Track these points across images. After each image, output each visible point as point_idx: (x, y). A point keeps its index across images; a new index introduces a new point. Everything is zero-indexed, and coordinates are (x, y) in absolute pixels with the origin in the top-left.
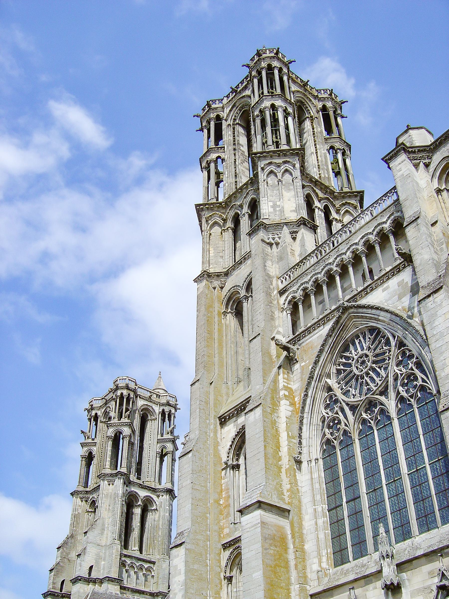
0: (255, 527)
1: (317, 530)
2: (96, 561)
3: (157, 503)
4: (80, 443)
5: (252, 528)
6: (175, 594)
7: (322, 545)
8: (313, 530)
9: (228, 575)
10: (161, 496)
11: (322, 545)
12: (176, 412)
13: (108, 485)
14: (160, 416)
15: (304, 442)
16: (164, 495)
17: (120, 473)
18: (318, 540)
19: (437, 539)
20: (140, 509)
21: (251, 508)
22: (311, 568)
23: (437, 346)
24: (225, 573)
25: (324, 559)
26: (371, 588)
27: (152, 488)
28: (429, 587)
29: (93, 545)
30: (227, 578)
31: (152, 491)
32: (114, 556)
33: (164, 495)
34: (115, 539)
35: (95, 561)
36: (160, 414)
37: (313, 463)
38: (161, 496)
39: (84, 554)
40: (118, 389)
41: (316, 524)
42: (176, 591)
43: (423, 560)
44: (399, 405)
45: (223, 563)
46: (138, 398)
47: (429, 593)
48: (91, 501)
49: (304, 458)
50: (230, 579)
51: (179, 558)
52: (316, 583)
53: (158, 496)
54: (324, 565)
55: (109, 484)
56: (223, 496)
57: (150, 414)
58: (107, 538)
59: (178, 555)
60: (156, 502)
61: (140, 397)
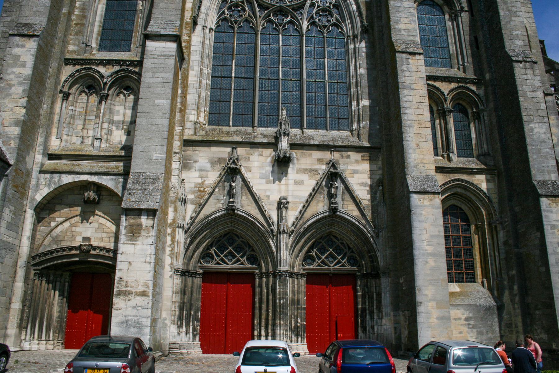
0: (167, 57)
1: (200, 87)
5: (162, 57)
6: (10, 86)
7: (202, 102)
8: (196, 85)
9: (66, 90)
11: (202, 102)
15: (203, 9)
18: (199, 97)
19: (320, 138)
21: (162, 38)
22: (189, 118)
23: (396, 5)
24: (63, 87)
25: (202, 115)
26: (256, 154)
28: (316, 170)
30: (64, 93)
37: (207, 31)
41: (201, 82)
42: (12, 83)
43: (316, 148)
44: (310, 27)
45: (63, 78)
47: (315, 174)
49: (200, 21)
50: (66, 96)
51: (24, 49)
52: (191, 132)
54: (201, 119)
56: (76, 13)
59: (23, 46)
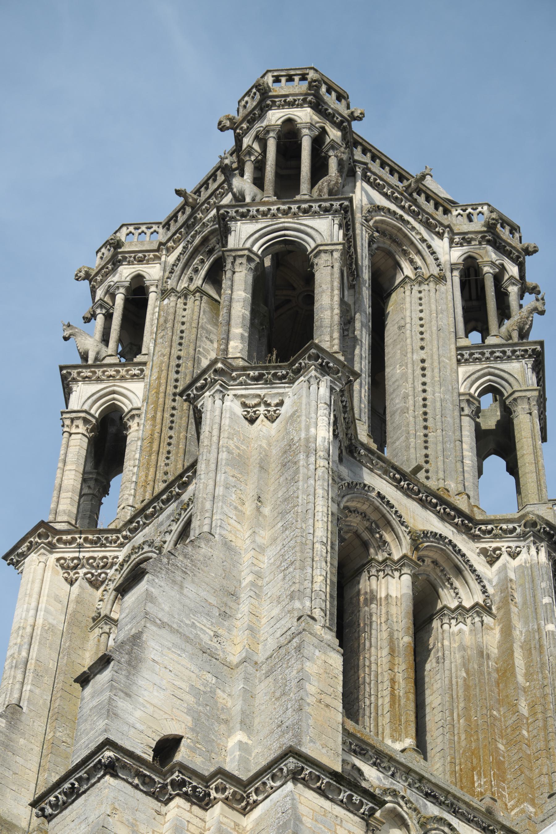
2: (197, 720)
4: (62, 368)
10: (505, 557)
16: (524, 550)
17: (317, 357)
20: (407, 579)
27: (460, 513)
29: (176, 639)
32: (311, 688)
33: (524, 550)
34: (313, 619)
36: (456, 273)
38: (505, 557)
39: (129, 663)
40: (269, 108)
55: (252, 421)
58: (252, 630)
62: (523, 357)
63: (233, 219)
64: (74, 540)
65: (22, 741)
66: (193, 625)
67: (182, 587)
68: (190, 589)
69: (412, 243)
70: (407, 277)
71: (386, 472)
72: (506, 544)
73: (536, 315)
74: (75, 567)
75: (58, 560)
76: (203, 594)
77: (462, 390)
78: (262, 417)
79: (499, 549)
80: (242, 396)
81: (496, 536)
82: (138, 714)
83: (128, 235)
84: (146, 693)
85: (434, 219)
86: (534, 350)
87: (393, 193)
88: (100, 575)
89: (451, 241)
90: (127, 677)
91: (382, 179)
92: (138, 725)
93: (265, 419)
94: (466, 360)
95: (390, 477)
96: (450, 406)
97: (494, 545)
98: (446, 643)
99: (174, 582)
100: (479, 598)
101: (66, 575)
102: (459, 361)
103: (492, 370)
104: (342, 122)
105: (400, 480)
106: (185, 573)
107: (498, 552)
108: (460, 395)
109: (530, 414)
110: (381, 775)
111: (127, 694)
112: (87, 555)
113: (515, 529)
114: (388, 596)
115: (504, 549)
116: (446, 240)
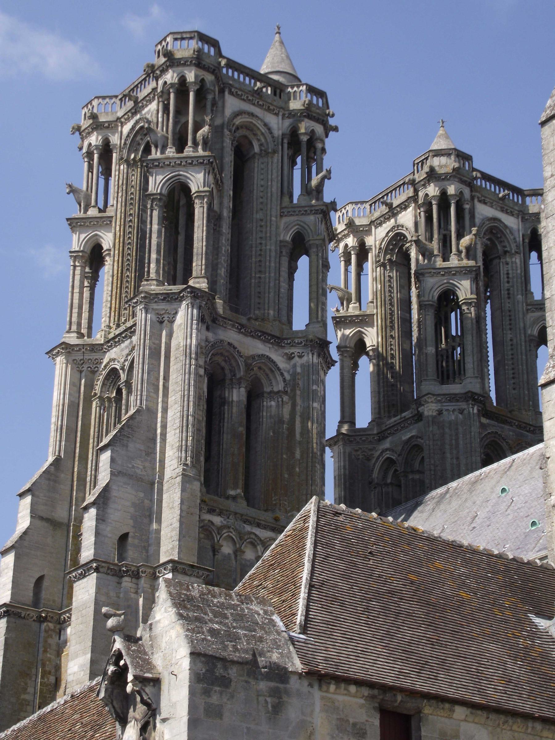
3: (288, 377)
12: (327, 136)
13: (158, 324)
14: (286, 146)
20: (243, 390)
27: (273, 336)
31: (272, 343)
35: (131, 522)
46: (226, 93)
48: (107, 370)
53: (290, 357)
57: (259, 140)
60: (286, 374)
61: (231, 93)
62: (317, 214)
63: (151, 168)
64: (80, 350)
65: (62, 475)
66: (133, 467)
67: (127, 447)
68: (131, 445)
69: (259, 129)
70: (255, 153)
71: (233, 326)
72: (298, 351)
73: (326, 180)
74: (82, 364)
75: (74, 360)
76: (138, 446)
77: (282, 238)
78: (166, 321)
79: (293, 353)
80: (156, 309)
81: (292, 346)
82: (109, 529)
83: (99, 104)
84: (112, 516)
85: (272, 105)
86: (322, 210)
87: (247, 97)
88: (95, 368)
89: (284, 115)
90: (103, 511)
91: (241, 90)
92: (109, 535)
93: (168, 323)
94: (286, 216)
95: (236, 328)
96: (273, 254)
97: (292, 351)
98: (265, 414)
99: (123, 445)
100: (281, 387)
101: (78, 369)
102: (281, 216)
103: (299, 223)
104: (214, 70)
105: (241, 329)
106: (129, 437)
107: (293, 355)
108: (281, 241)
109: (317, 255)
110: (222, 519)
111: (103, 521)
112: (88, 357)
113: (301, 343)
114: (232, 401)
115: (296, 353)
116: (280, 117)
